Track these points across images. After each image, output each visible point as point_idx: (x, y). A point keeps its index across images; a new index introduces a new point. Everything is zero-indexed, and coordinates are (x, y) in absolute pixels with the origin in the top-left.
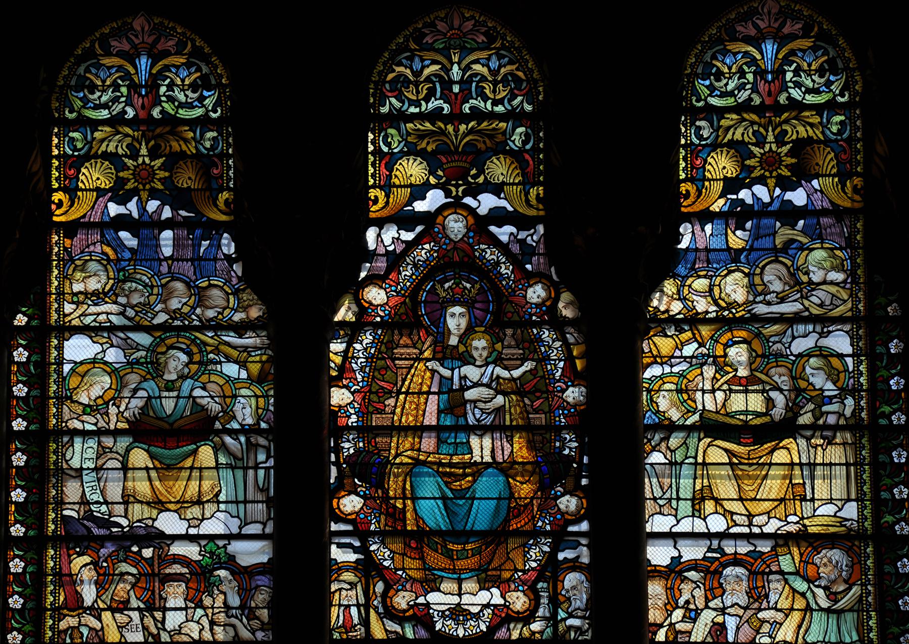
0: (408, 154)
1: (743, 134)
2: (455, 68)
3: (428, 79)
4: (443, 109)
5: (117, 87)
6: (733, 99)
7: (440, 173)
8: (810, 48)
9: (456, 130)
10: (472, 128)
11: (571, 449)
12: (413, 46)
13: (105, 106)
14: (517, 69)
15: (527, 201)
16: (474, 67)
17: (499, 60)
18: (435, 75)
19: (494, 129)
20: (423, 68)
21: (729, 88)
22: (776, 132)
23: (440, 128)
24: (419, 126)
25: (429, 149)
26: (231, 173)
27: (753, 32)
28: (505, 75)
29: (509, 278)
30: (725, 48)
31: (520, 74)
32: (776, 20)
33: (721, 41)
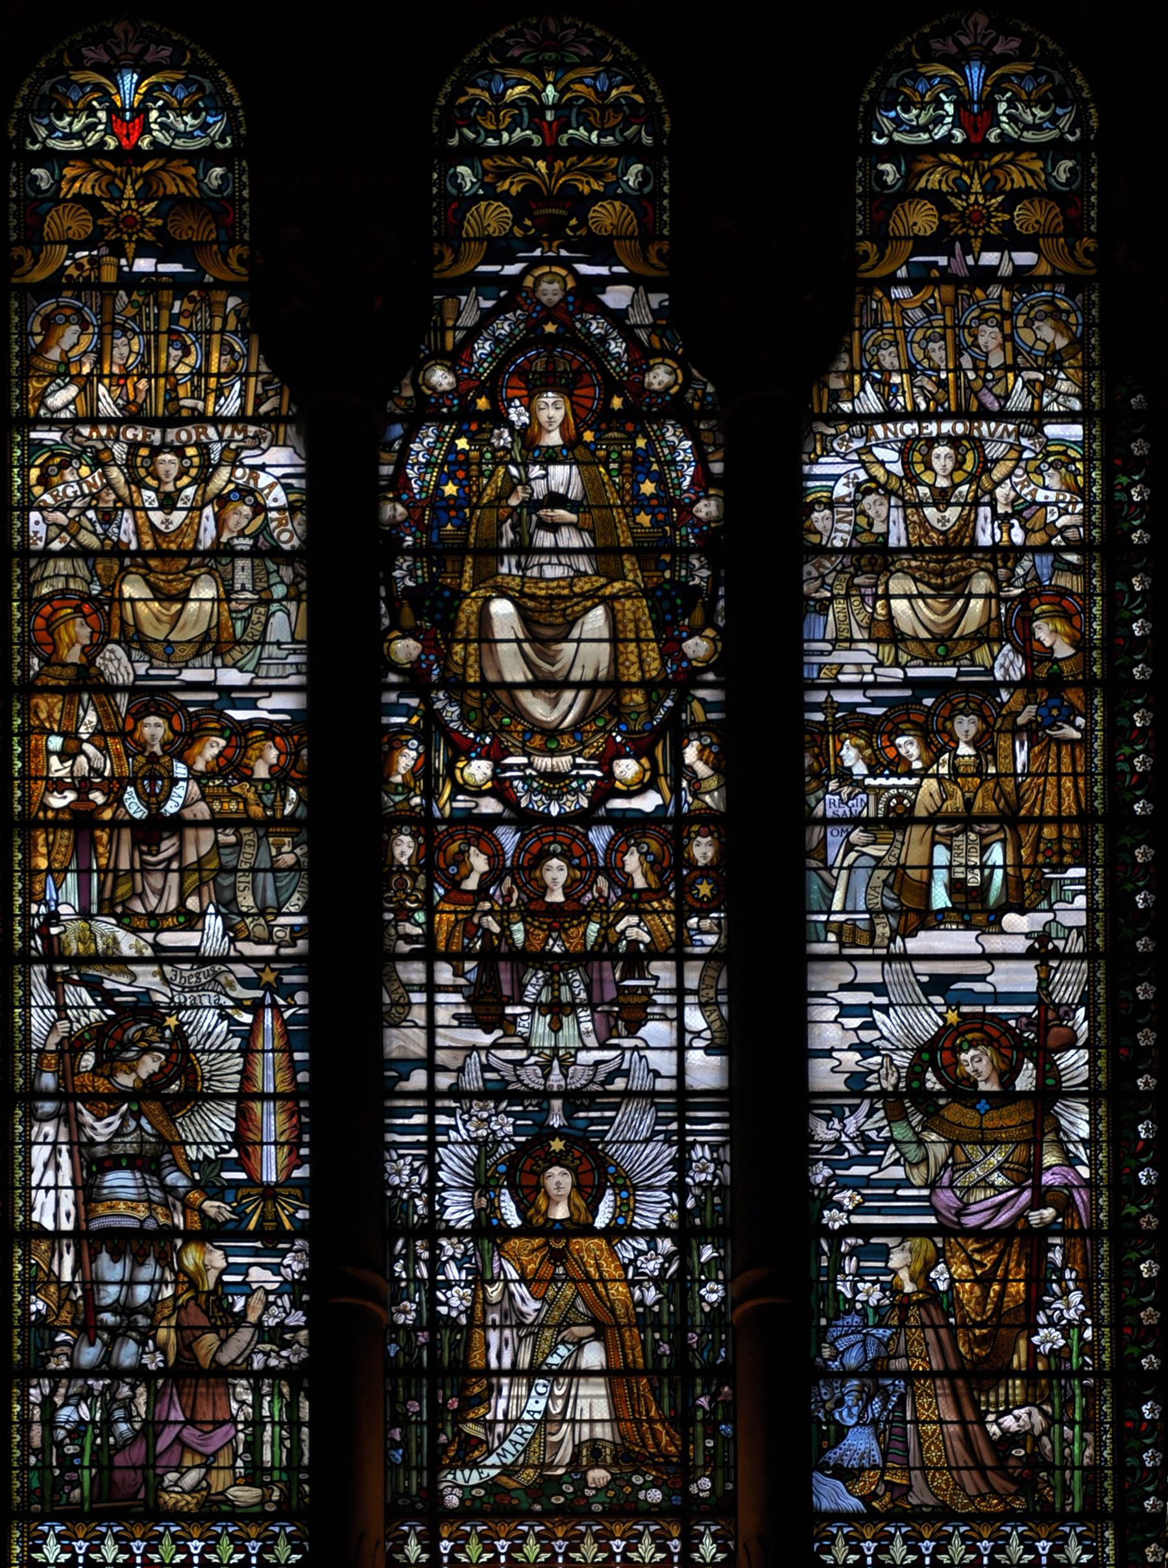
0: (484, 198)
1: (940, 182)
2: (550, 90)
4: (532, 141)
5: (92, 112)
6: (926, 136)
7: (528, 222)
8: (1028, 73)
9: (550, 168)
10: (572, 165)
11: (702, 578)
12: (492, 60)
13: (78, 136)
14: (634, 91)
15: (646, 259)
16: (577, 87)
17: (610, 79)
19: (601, 167)
20: (505, 90)
21: (922, 121)
22: (984, 180)
23: (528, 165)
24: (499, 162)
25: (514, 191)
26: (246, 222)
27: (954, 50)
28: (617, 98)
29: (620, 358)
30: (915, 71)
31: (638, 98)
32: (985, 36)
33: (912, 63)
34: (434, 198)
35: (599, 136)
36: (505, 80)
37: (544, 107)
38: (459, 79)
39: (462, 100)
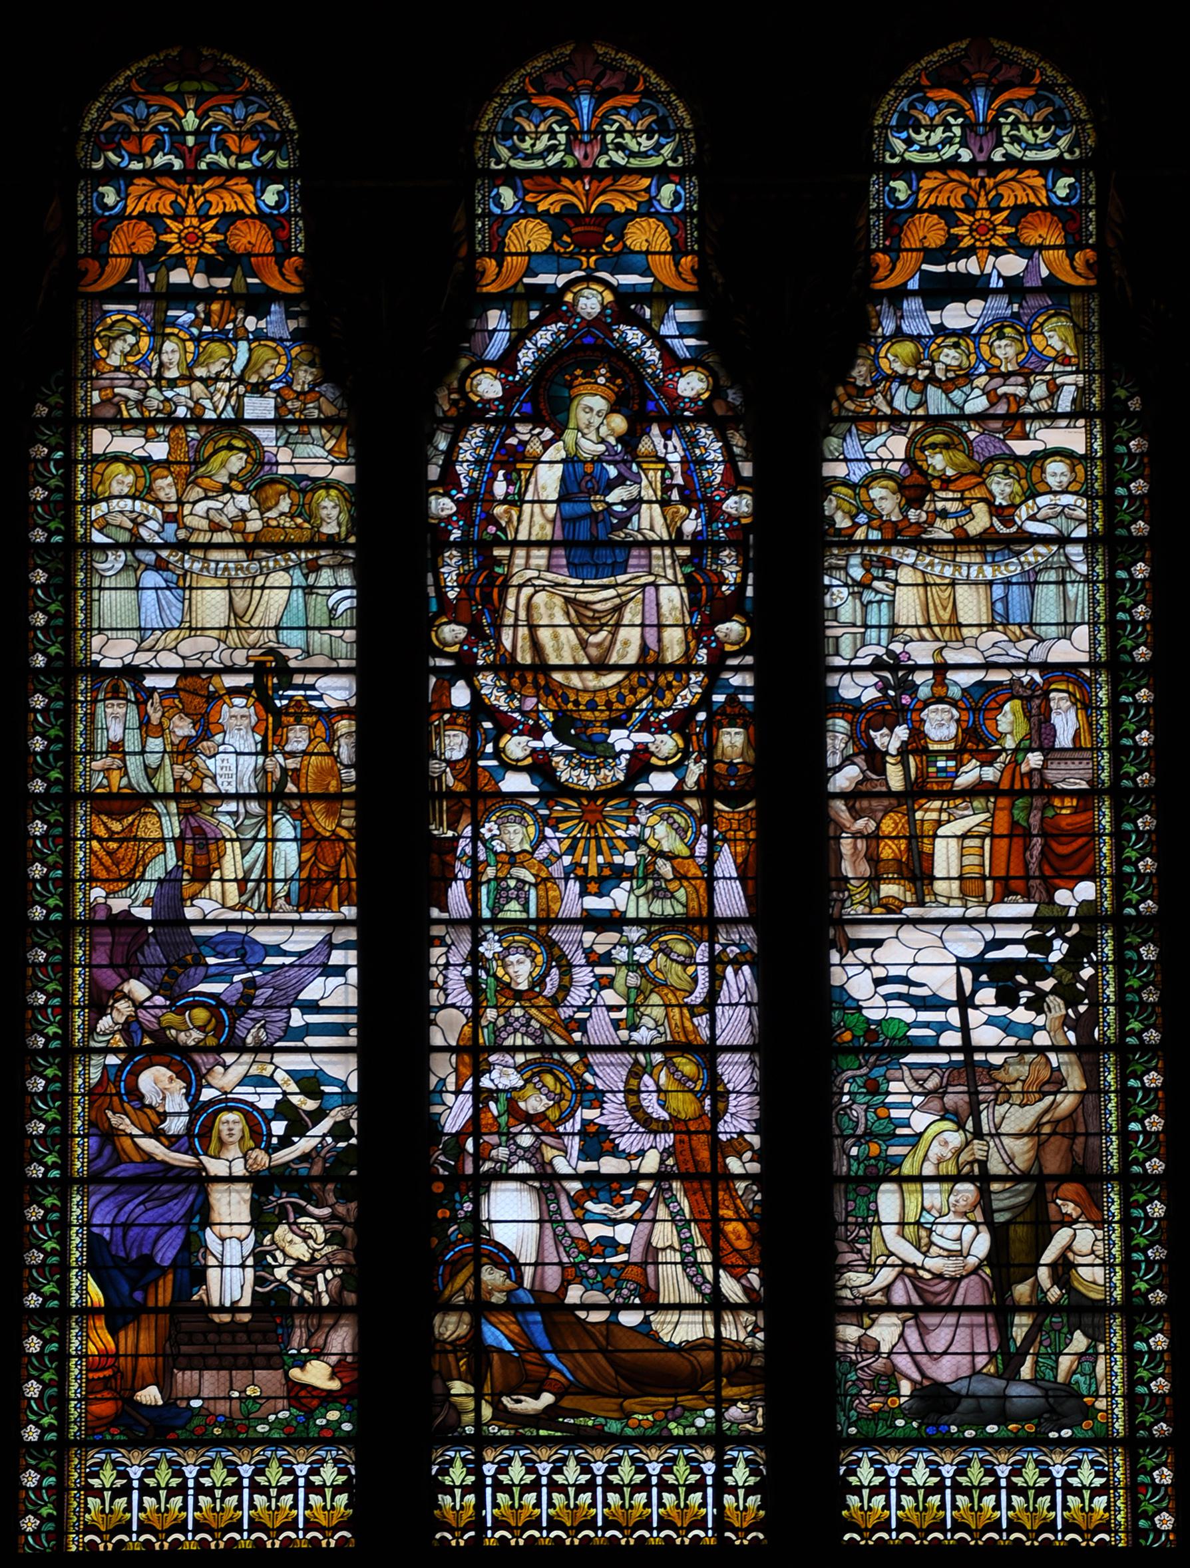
3: (154, 130)
14: (270, 118)
18: (165, 124)
31: (274, 124)
34: (82, 217)
35: (237, 161)
36: (148, 107)
37: (185, 133)
38: (105, 105)
39: (107, 125)
